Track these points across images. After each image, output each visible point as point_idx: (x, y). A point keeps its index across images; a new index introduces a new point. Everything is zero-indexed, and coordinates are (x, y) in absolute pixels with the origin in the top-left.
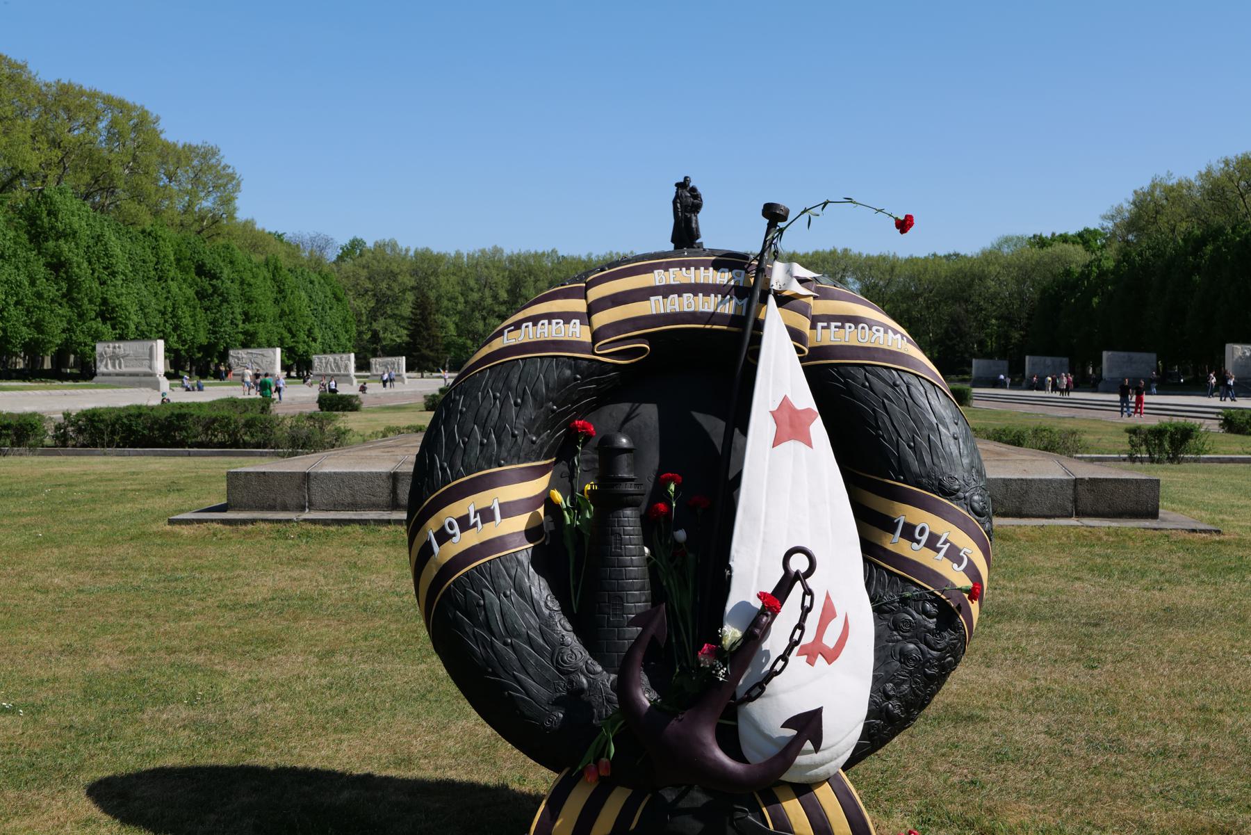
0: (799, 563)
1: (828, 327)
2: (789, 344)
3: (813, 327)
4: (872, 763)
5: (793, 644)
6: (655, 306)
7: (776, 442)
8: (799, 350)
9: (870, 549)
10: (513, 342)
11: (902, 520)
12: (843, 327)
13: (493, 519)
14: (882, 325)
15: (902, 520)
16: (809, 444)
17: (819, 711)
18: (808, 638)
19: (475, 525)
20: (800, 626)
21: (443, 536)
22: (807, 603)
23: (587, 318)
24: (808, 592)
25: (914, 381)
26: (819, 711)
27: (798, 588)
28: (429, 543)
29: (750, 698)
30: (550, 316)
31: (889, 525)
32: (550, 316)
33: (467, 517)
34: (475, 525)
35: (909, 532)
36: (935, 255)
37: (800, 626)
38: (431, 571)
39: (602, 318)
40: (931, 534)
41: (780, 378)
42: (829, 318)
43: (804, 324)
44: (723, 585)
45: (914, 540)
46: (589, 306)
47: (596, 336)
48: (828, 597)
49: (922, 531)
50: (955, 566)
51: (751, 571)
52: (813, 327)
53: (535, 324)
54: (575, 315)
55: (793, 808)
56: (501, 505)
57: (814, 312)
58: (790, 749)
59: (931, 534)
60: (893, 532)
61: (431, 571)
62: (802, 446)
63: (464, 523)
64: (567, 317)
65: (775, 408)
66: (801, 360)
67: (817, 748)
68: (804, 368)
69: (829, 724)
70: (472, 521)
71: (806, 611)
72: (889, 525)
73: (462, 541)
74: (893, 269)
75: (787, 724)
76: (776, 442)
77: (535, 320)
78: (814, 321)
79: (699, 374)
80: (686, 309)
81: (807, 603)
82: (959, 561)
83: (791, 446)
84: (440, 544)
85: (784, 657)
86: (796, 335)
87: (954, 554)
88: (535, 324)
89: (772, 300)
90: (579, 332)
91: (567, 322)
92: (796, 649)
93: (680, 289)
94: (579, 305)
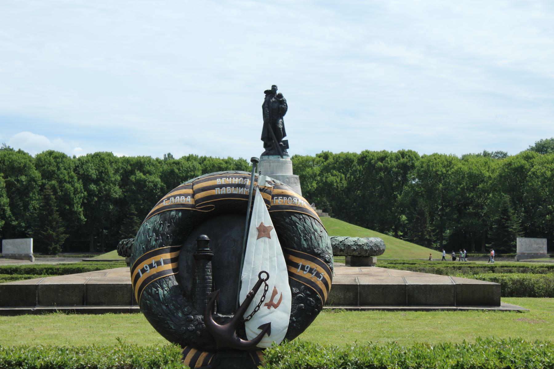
0: (264, 276)
1: (278, 199)
2: (264, 206)
3: (273, 198)
5: (262, 302)
6: (217, 191)
8: (267, 206)
9: (290, 274)
10: (167, 204)
11: (301, 264)
12: (283, 199)
13: (161, 264)
15: (301, 264)
16: (270, 238)
17: (270, 323)
18: (267, 300)
19: (155, 267)
20: (264, 296)
21: (143, 271)
22: (266, 289)
24: (266, 285)
25: (307, 217)
26: (270, 323)
27: (263, 284)
28: (138, 274)
29: (247, 320)
30: (180, 195)
31: (296, 266)
32: (180, 195)
33: (152, 264)
34: (155, 267)
37: (264, 296)
39: (199, 196)
40: (310, 268)
41: (261, 215)
42: (278, 195)
45: (304, 270)
46: (194, 192)
47: (197, 202)
48: (275, 287)
49: (308, 267)
50: (318, 279)
51: (248, 277)
52: (273, 198)
53: (175, 198)
54: (188, 195)
56: (164, 260)
57: (272, 193)
58: (260, 338)
59: (310, 268)
60: (298, 268)
62: (267, 239)
63: (151, 266)
64: (186, 195)
65: (258, 226)
67: (269, 334)
68: (270, 213)
70: (154, 265)
71: (266, 291)
72: (296, 266)
73: (150, 272)
75: (260, 328)
77: (175, 197)
79: (230, 212)
80: (228, 193)
81: (266, 289)
82: (320, 277)
84: (143, 273)
85: (259, 306)
86: (266, 201)
87: (318, 275)
88: (175, 198)
89: (258, 191)
90: (189, 200)
91: (186, 197)
92: (263, 303)
93: (226, 186)
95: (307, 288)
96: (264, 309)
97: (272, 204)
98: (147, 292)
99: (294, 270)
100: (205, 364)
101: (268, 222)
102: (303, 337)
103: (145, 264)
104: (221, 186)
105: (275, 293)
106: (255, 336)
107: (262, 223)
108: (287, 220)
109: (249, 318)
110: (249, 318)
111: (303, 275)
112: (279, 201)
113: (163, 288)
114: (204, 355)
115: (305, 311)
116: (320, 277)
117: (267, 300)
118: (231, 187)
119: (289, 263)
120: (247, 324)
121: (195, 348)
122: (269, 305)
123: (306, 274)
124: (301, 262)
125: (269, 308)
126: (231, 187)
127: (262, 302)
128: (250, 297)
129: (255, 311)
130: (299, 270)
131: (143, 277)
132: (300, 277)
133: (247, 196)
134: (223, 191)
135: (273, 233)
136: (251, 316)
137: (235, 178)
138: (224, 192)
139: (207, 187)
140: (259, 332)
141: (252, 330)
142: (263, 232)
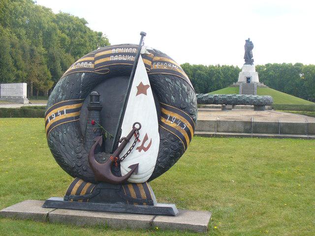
0: (137, 126)
2: (144, 68)
3: (152, 64)
4: (157, 180)
5: (133, 146)
6: (111, 58)
7: (137, 94)
9: (160, 123)
14: (170, 63)
21: (51, 118)
23: (93, 62)
28: (48, 120)
29: (121, 161)
31: (166, 117)
32: (84, 61)
35: (171, 119)
36: (100, 34)
38: (49, 125)
39: (97, 62)
42: (157, 62)
43: (149, 63)
44: (119, 131)
45: (171, 121)
47: (96, 66)
50: (182, 128)
52: (152, 64)
55: (131, 189)
56: (66, 110)
61: (49, 125)
63: (57, 115)
64: (88, 62)
66: (148, 73)
69: (141, 169)
72: (166, 117)
73: (55, 119)
74: (48, 35)
75: (130, 167)
76: (137, 94)
78: (153, 62)
83: (142, 95)
90: (91, 65)
93: (118, 54)
94: (92, 59)
95: (172, 135)
96: (135, 152)
97: (152, 68)
98: (52, 134)
99: (163, 120)
100: (87, 193)
101: (146, 82)
102: (171, 173)
103: (52, 113)
104: (114, 55)
105: (146, 138)
106: (126, 173)
107: (141, 83)
108: (162, 81)
109: (122, 159)
110: (122, 159)
111: (170, 125)
112: (157, 66)
113: (62, 132)
114: (88, 185)
115: (172, 151)
116: (183, 127)
117: (139, 144)
118: (122, 55)
119: (161, 115)
120: (121, 163)
121: (83, 179)
122: (140, 149)
123: (172, 124)
124: (169, 114)
125: (140, 151)
126: (122, 55)
127: (133, 146)
128: (127, 140)
129: (127, 154)
130: (167, 121)
131: (50, 122)
132: (167, 126)
133: (132, 62)
134: (116, 58)
135: (149, 91)
136: (124, 157)
137: (126, 48)
138: (117, 59)
139: (104, 55)
140: (129, 170)
141: (125, 169)
142: (142, 89)
